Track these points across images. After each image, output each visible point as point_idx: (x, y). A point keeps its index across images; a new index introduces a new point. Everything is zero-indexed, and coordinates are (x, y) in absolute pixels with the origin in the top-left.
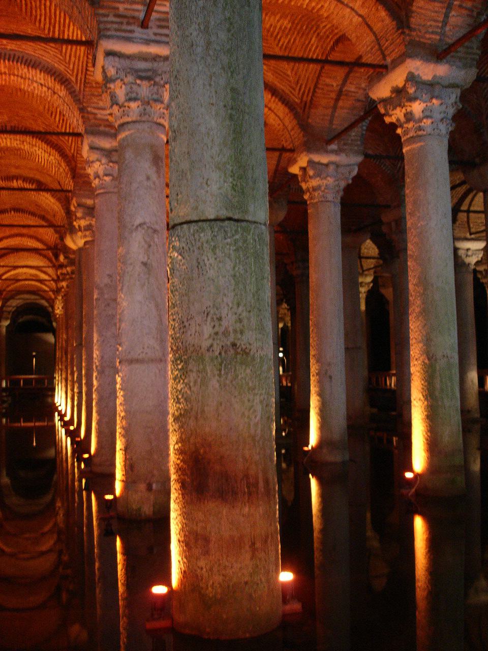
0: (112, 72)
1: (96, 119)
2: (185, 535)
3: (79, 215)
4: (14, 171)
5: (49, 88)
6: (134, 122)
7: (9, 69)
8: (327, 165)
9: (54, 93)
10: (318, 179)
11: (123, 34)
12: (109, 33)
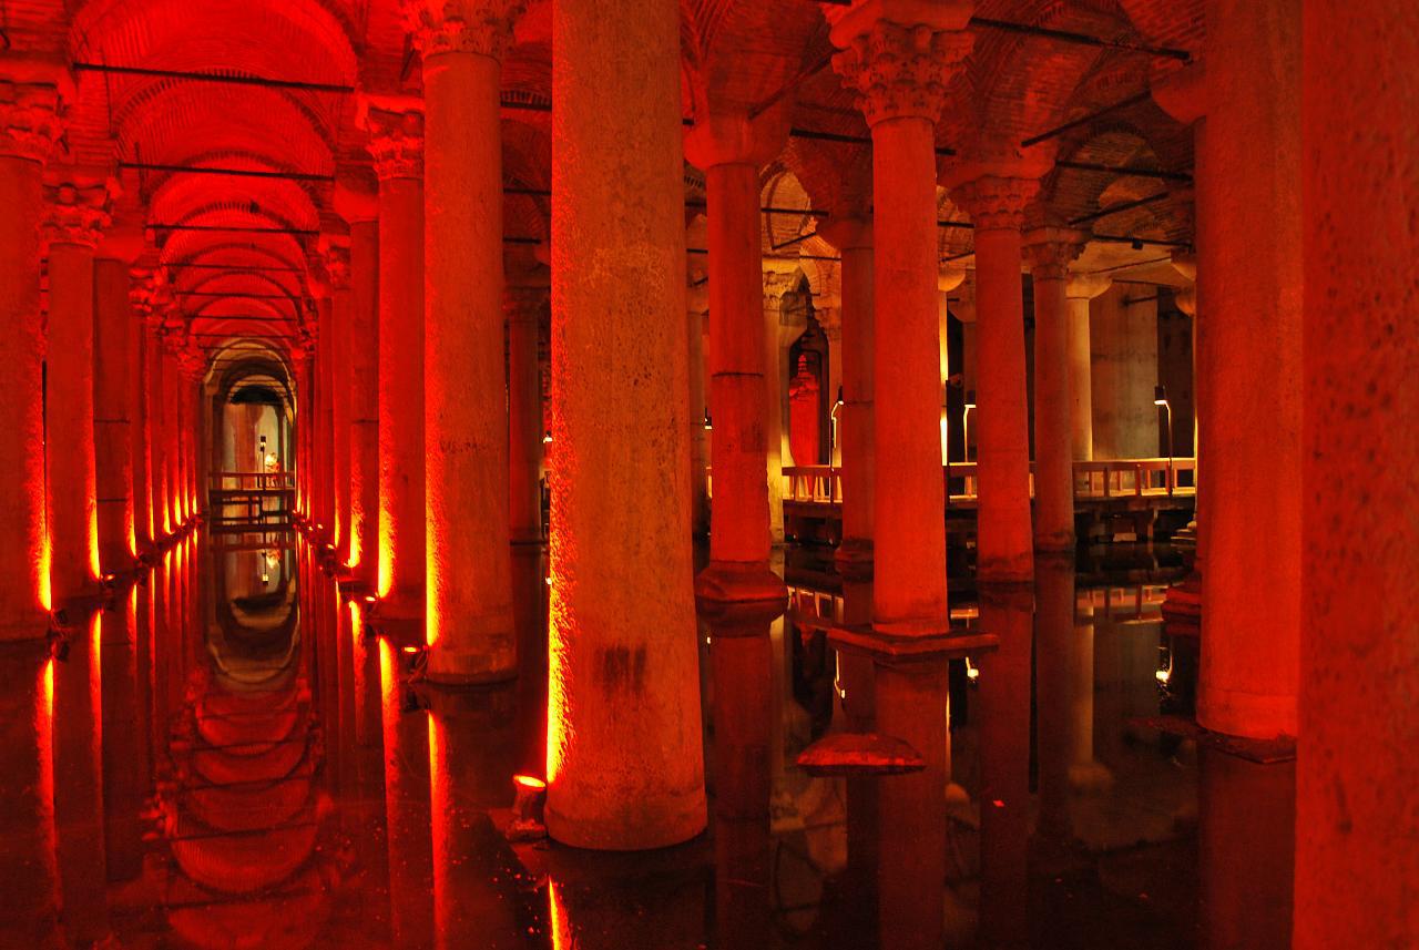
8: (402, 116)
10: (386, 138)
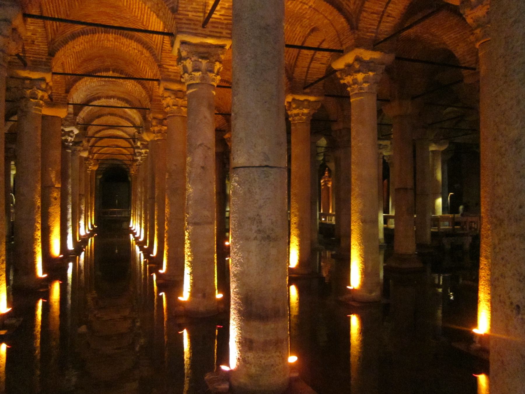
0: (184, 54)
1: (169, 72)
2: (239, 339)
3: (154, 123)
4: (111, 93)
5: (139, 51)
6: (197, 84)
7: (115, 39)
9: (142, 54)
11: (191, 31)
12: (183, 30)
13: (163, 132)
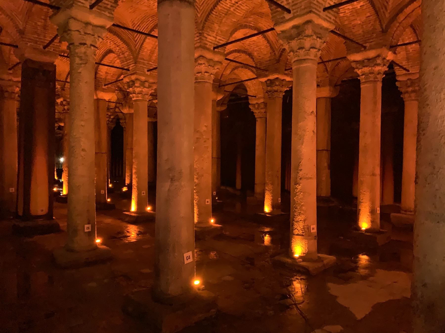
6: (312, 59)
13: (144, 94)
